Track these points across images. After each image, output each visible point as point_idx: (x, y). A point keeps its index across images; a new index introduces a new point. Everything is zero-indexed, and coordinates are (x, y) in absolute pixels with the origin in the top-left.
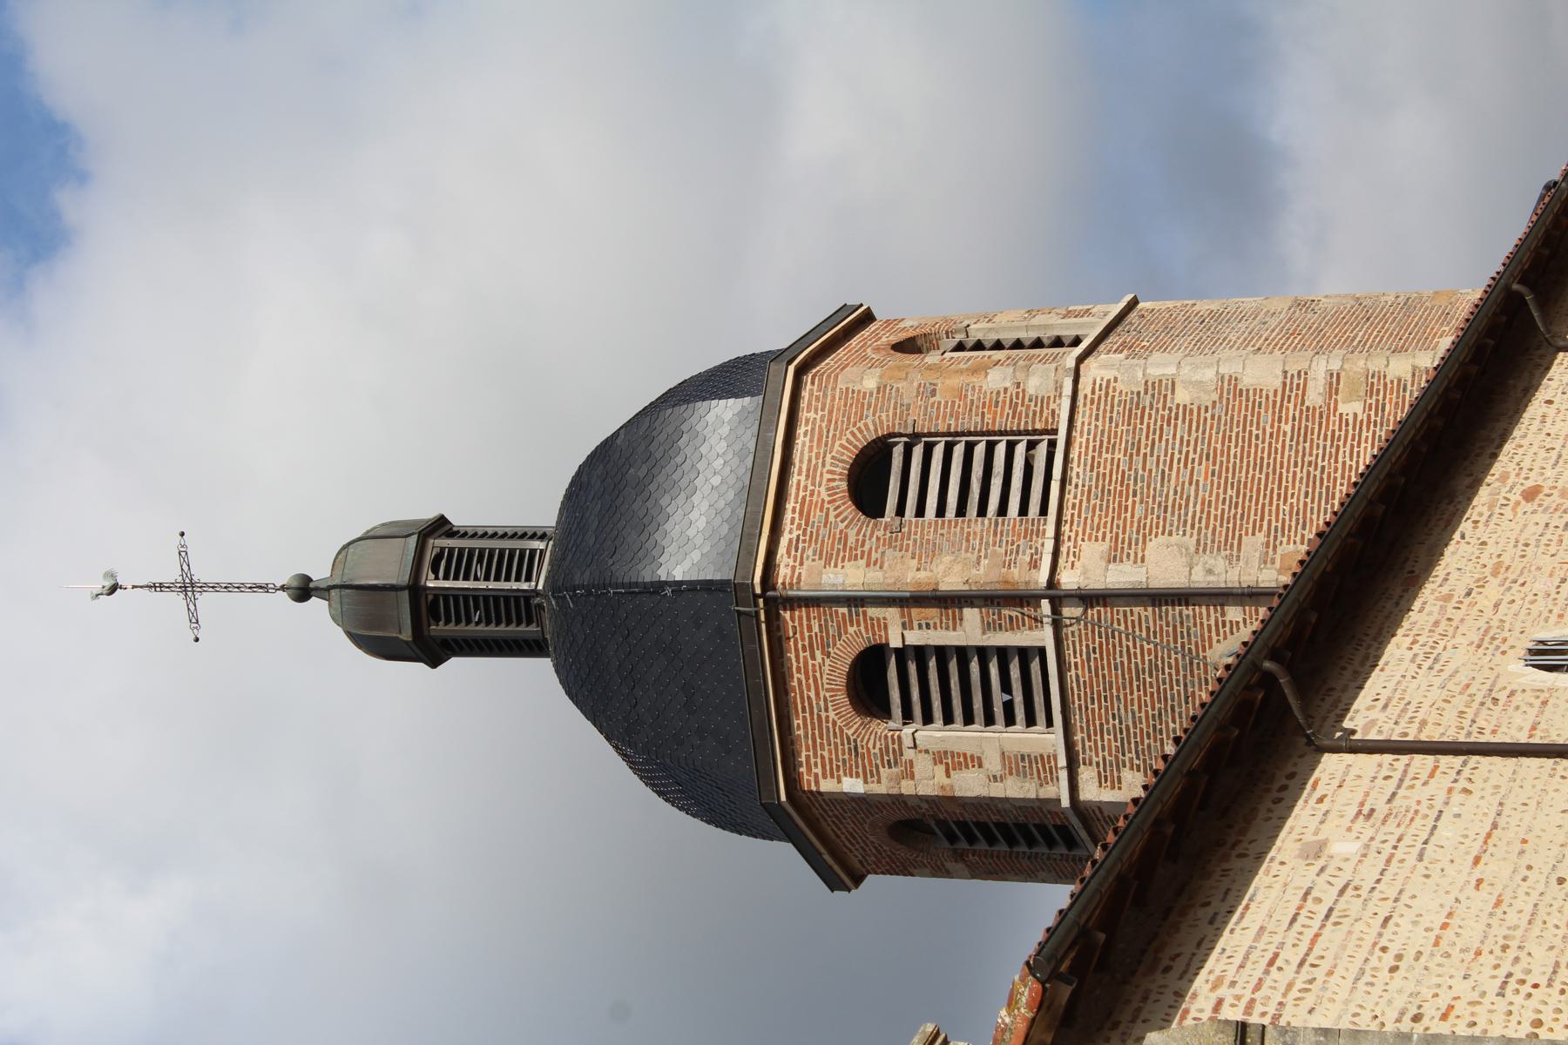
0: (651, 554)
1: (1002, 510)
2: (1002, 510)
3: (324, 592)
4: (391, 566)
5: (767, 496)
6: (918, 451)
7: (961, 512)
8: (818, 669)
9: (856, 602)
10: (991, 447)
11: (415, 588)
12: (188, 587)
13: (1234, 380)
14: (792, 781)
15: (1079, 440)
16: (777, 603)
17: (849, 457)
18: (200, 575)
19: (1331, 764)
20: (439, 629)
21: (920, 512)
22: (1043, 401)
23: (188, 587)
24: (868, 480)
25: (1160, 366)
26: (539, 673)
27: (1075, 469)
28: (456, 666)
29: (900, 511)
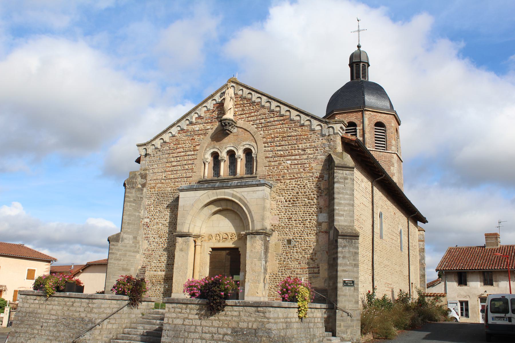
0: (369, 94)
1: (376, 143)
2: (376, 143)
3: (359, 49)
4: (363, 59)
5: (377, 110)
6: (383, 131)
7: (376, 137)
8: (353, 117)
9: (363, 123)
10: (384, 141)
11: (360, 62)
12: (359, 31)
13: (394, 175)
14: (337, 114)
15: (386, 154)
16: (362, 112)
17: (383, 122)
18: (360, 32)
19: (370, 184)
20: (355, 65)
21: (375, 132)
22: (391, 149)
23: (359, 31)
24: (379, 124)
25: (396, 165)
26: (348, 80)
27: (382, 153)
28: (349, 69)
29: (376, 129)
